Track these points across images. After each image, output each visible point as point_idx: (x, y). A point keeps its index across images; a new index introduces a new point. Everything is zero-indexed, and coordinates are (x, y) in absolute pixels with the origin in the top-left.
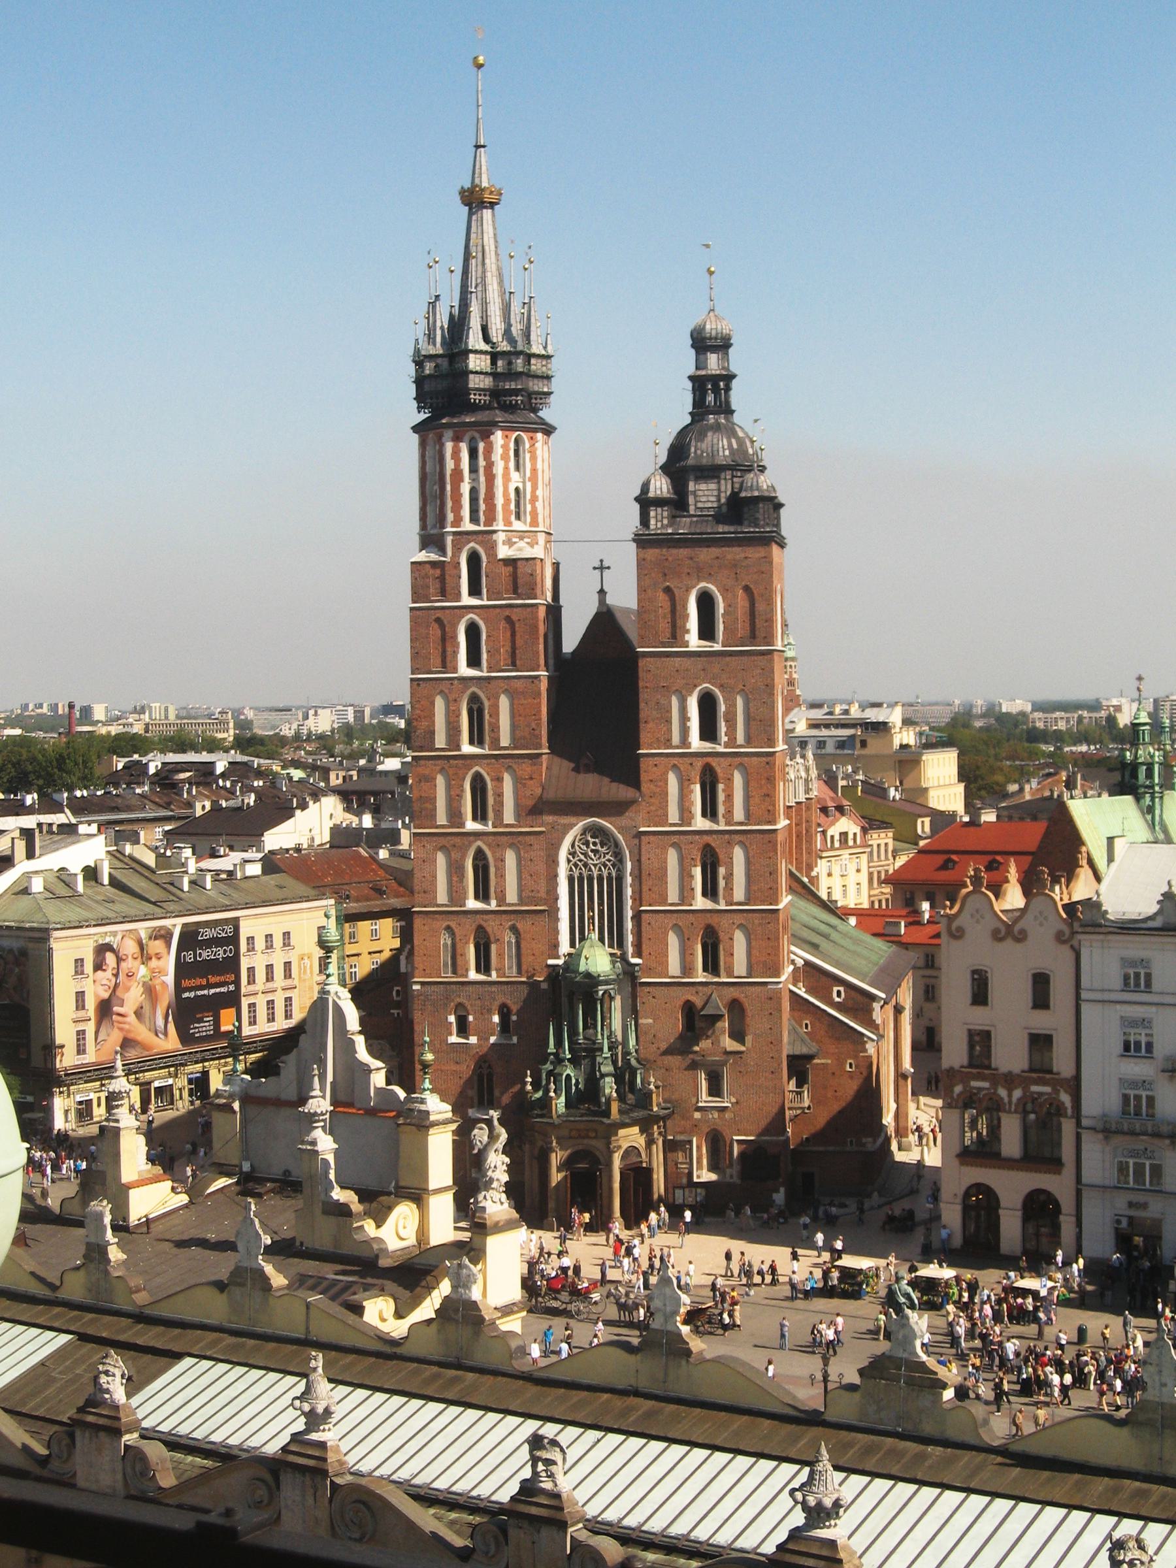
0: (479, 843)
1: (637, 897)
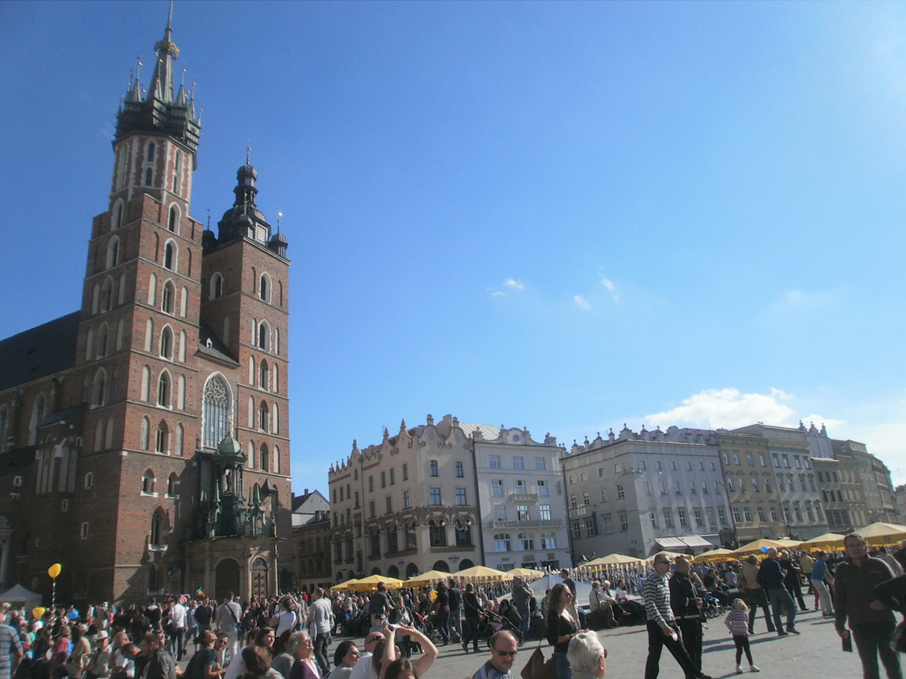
0: (165, 369)
1: (236, 421)
